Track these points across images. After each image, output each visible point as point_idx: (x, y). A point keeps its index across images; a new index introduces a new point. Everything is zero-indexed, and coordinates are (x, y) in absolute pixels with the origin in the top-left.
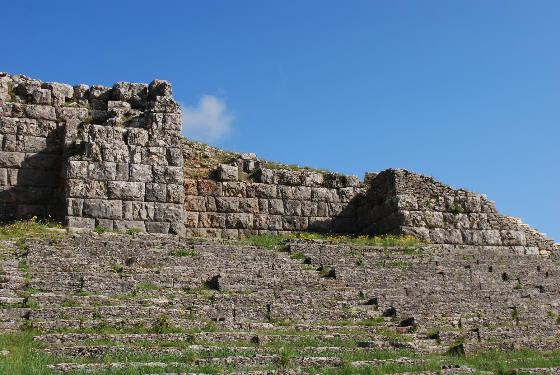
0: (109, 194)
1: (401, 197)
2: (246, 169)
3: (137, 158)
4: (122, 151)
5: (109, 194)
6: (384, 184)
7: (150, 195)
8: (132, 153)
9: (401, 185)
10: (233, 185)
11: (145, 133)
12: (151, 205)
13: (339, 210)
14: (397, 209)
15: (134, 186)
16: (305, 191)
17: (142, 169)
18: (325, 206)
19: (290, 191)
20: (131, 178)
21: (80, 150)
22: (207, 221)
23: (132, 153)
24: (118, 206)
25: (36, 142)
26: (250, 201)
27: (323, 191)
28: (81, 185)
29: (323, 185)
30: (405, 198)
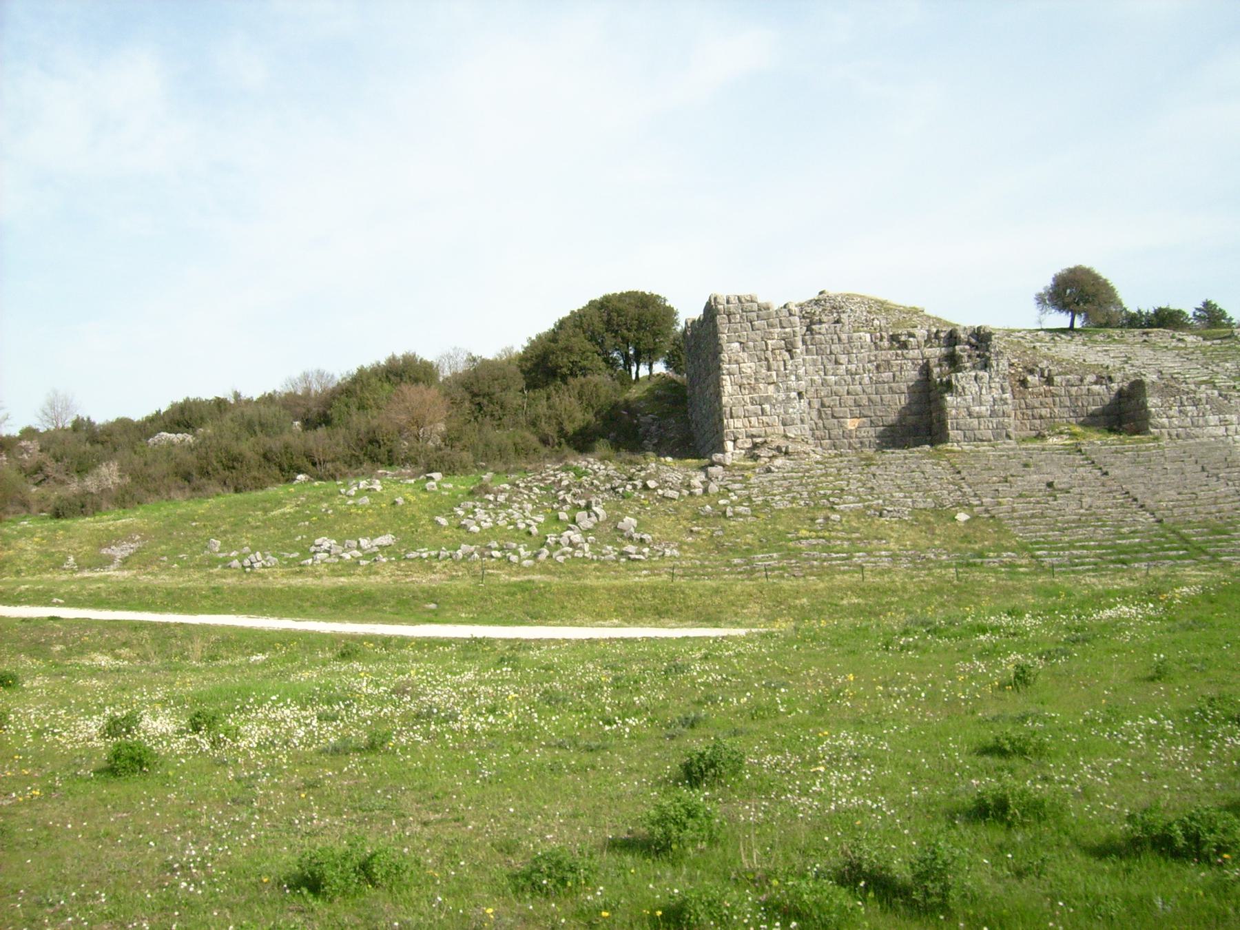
0: (970, 415)
1: (1149, 399)
2: (1042, 376)
3: (984, 391)
4: (974, 388)
5: (970, 415)
6: (1135, 390)
7: (993, 414)
8: (981, 389)
9: (1149, 391)
10: (1036, 390)
11: (987, 375)
12: (995, 421)
13: (1107, 401)
14: (1146, 408)
15: (983, 408)
16: (1084, 388)
17: (987, 398)
18: (1098, 398)
19: (1074, 390)
20: (981, 404)
21: (949, 387)
22: (1019, 416)
23: (981, 389)
24: (976, 422)
25: (912, 374)
26: (1047, 400)
27: (1096, 388)
28: (954, 412)
29: (1096, 383)
30: (1153, 402)
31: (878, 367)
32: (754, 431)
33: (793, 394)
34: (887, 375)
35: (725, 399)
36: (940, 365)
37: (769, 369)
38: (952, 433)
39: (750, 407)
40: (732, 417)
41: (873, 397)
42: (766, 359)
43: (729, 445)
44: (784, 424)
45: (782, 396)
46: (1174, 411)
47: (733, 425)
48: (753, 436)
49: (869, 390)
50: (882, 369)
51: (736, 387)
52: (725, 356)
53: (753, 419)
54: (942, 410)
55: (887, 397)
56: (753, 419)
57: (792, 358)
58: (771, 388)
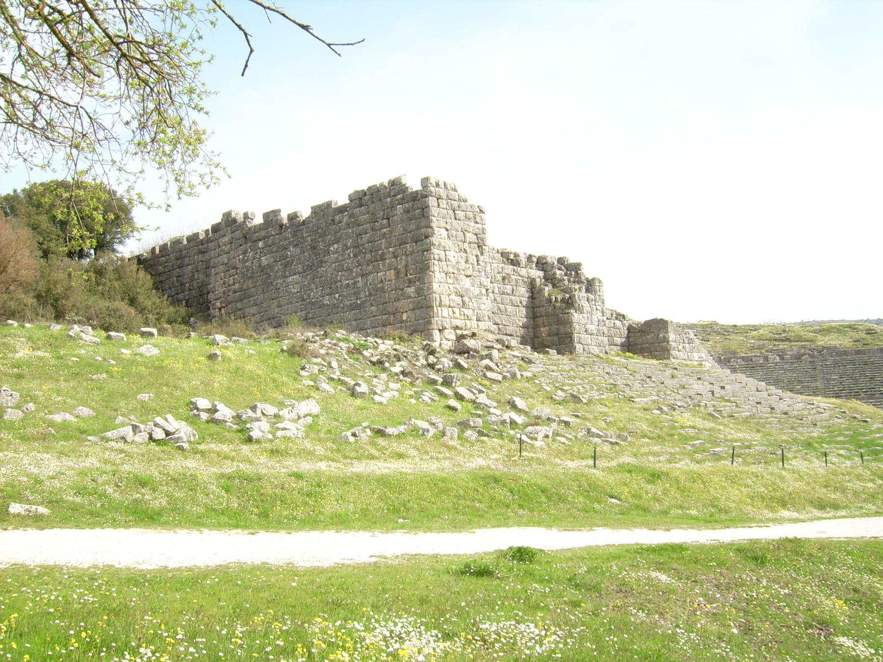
17: (595, 318)
25: (523, 291)
27: (617, 322)
30: (672, 336)
31: (504, 279)
32: (459, 323)
33: (484, 291)
34: (509, 288)
35: (435, 286)
36: (547, 286)
37: (467, 262)
38: (579, 347)
39: (453, 297)
40: (440, 305)
41: (501, 306)
42: (465, 251)
43: (436, 335)
44: (478, 320)
45: (477, 292)
46: (680, 347)
47: (442, 315)
48: (457, 328)
49: (498, 299)
50: (506, 281)
51: (443, 275)
52: (435, 240)
53: (457, 310)
54: (569, 323)
55: (510, 308)
56: (457, 310)
57: (482, 254)
58: (468, 279)
